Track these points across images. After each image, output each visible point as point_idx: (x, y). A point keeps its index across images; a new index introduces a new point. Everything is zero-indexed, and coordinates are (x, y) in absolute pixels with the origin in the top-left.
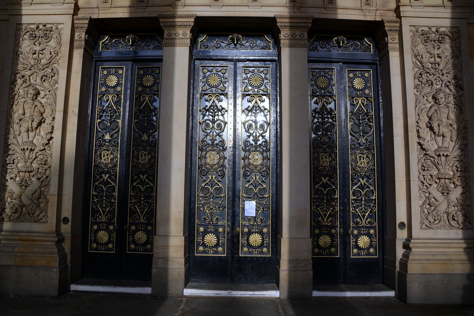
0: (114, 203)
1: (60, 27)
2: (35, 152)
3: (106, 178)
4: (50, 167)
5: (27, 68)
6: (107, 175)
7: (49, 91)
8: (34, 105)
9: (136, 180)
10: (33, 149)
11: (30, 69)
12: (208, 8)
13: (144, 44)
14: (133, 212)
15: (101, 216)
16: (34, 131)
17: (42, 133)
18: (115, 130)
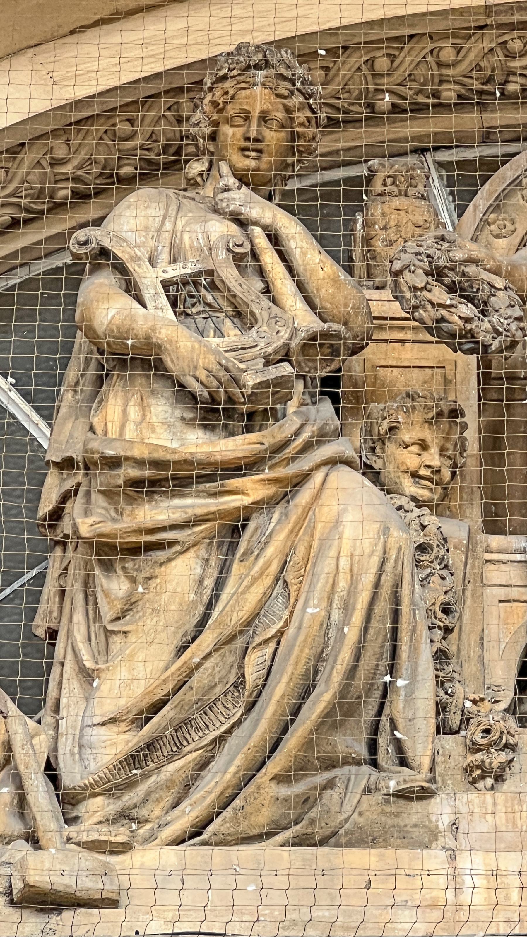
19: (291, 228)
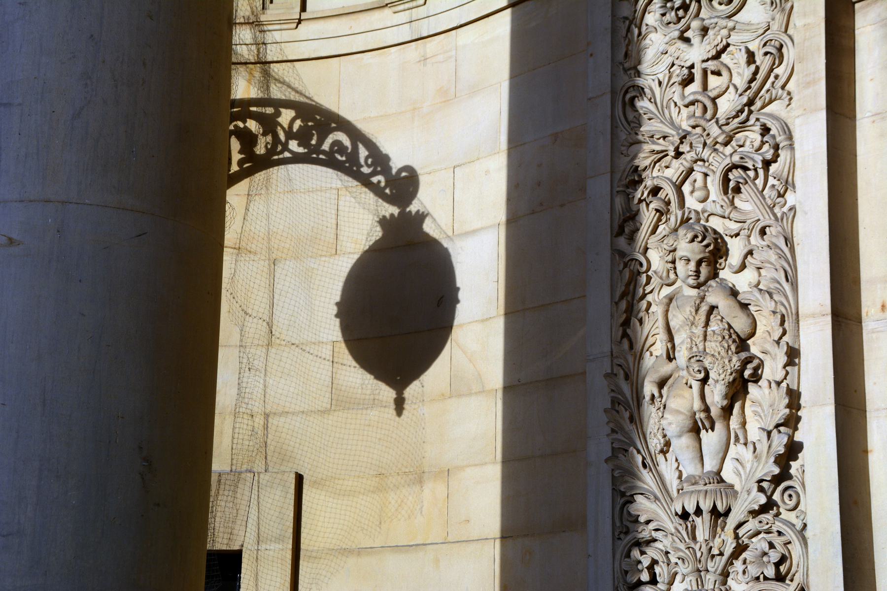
7: (763, 232)
8: (704, 308)
10: (721, 508)
11: (678, 154)
16: (719, 426)
17: (754, 432)
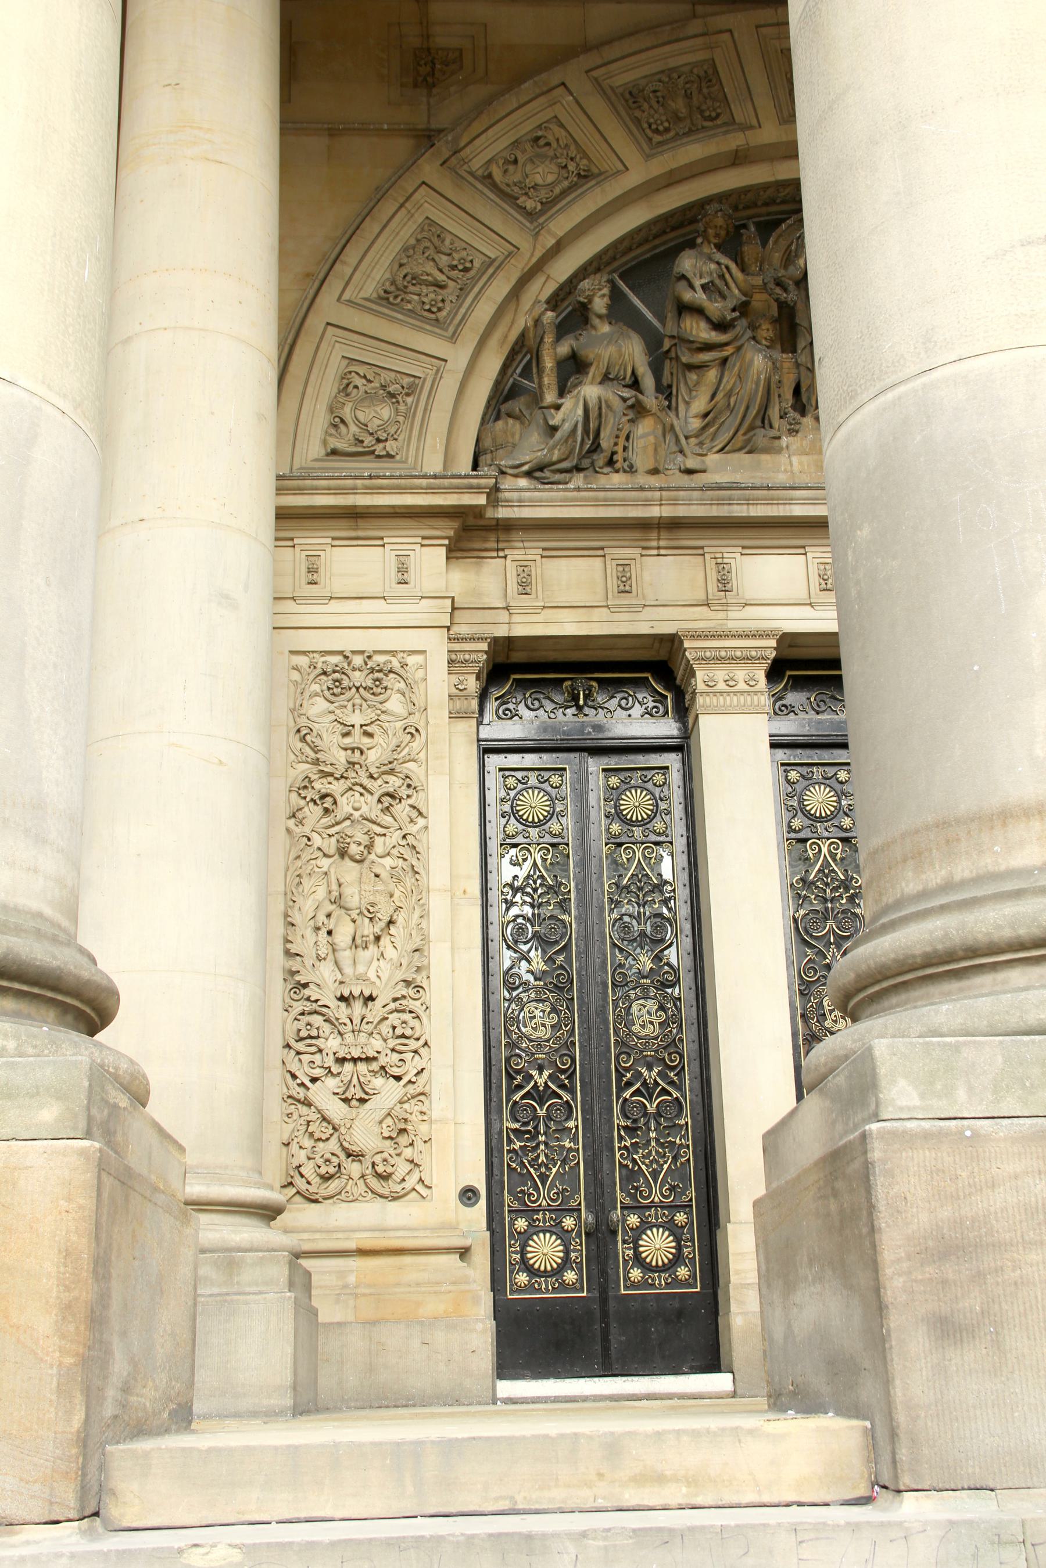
0: (570, 1149)
1: (411, 660)
2: (379, 1003)
3: (541, 1082)
4: (426, 1043)
5: (331, 775)
6: (546, 1073)
9: (629, 1084)
12: (807, 611)
13: (614, 702)
14: (631, 1175)
15: (537, 1189)
18: (557, 942)
19: (733, 266)
